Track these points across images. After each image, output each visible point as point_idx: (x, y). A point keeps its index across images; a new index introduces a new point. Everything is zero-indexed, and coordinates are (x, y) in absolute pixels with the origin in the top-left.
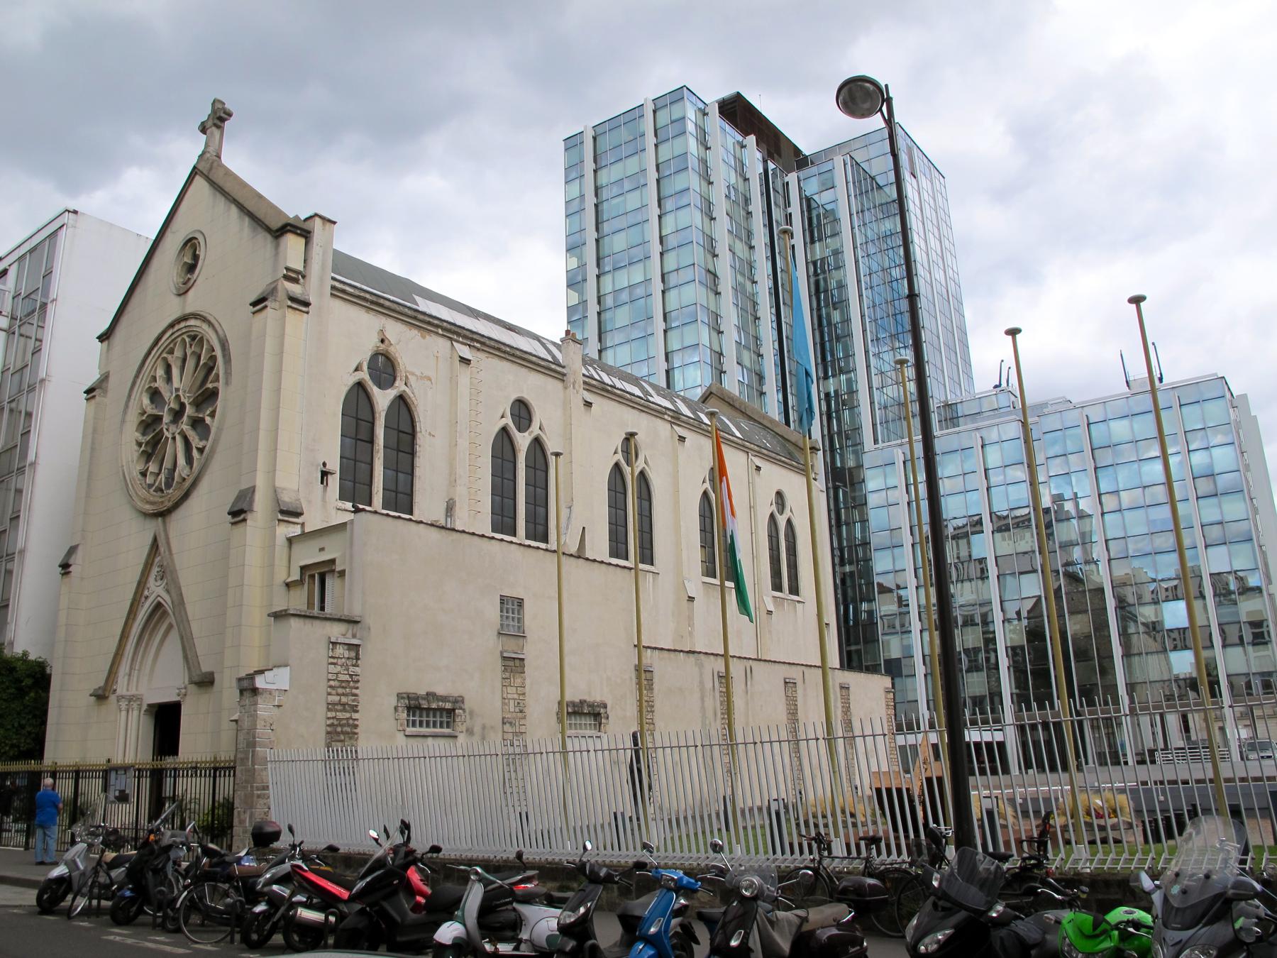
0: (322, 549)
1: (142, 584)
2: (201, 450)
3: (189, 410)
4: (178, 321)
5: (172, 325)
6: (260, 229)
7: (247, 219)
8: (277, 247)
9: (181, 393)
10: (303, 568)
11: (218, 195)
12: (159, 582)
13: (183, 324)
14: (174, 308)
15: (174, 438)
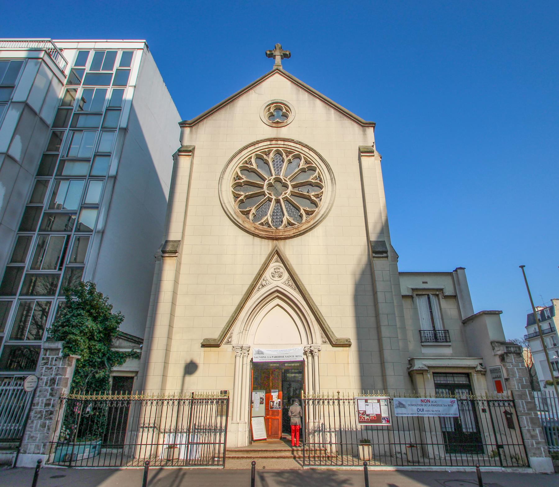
0: (426, 283)
1: (260, 275)
2: (308, 213)
3: (290, 188)
4: (277, 139)
5: (271, 140)
6: (345, 118)
7: (332, 111)
8: (364, 131)
9: (281, 177)
10: (413, 290)
11: (301, 89)
12: (276, 278)
13: (282, 143)
14: (271, 132)
15: (278, 201)
